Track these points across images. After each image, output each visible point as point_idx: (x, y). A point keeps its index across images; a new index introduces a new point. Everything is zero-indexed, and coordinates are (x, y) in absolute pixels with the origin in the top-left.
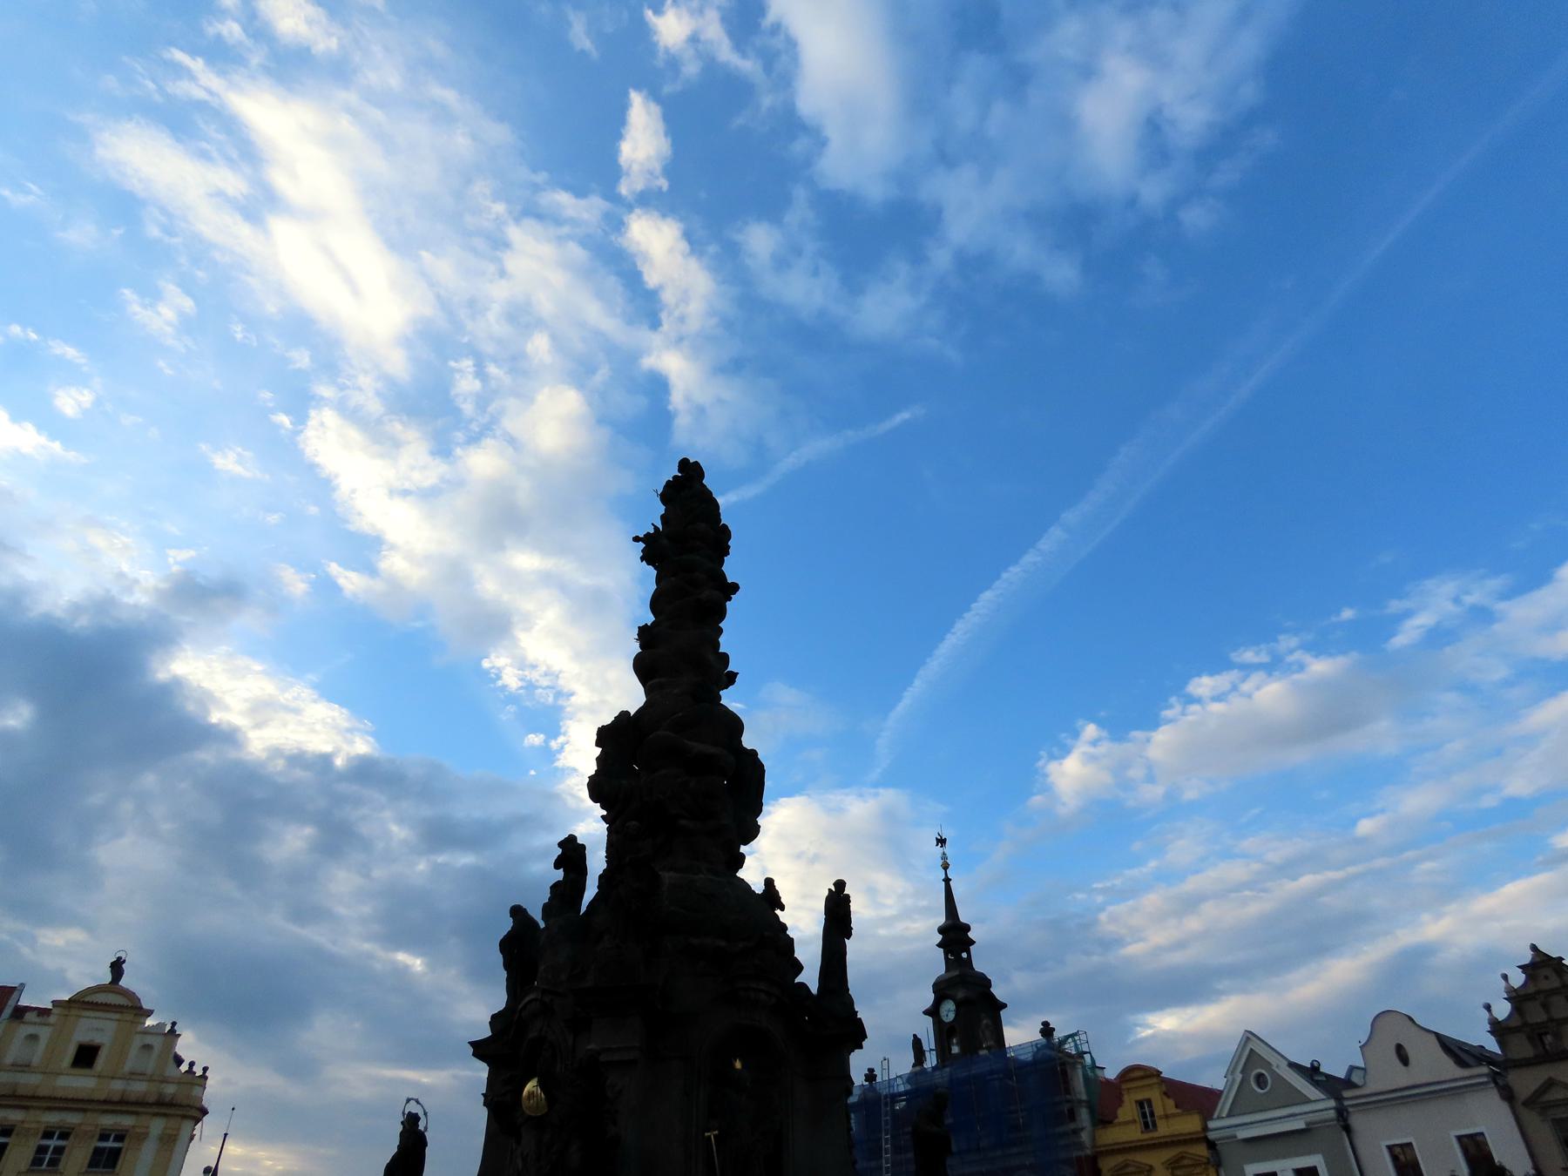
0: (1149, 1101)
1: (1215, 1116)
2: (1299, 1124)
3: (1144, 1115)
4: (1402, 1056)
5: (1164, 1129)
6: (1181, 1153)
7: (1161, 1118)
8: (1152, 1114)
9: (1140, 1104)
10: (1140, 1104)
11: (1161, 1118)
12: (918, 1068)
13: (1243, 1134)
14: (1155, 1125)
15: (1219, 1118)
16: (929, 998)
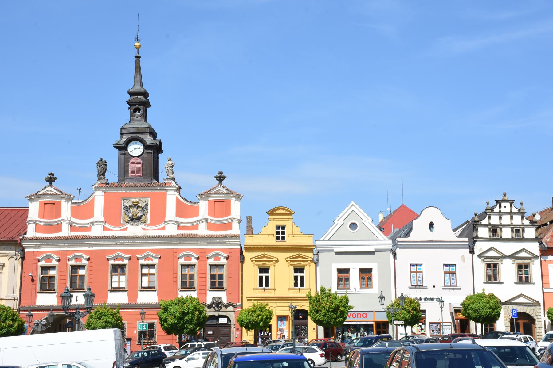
0: (283, 228)
1: (321, 239)
2: (372, 249)
3: (278, 233)
4: (432, 225)
5: (289, 241)
6: (299, 254)
7: (289, 235)
8: (283, 233)
9: (278, 227)
10: (278, 227)
11: (289, 235)
12: (104, 182)
13: (337, 250)
14: (283, 238)
15: (323, 240)
16: (117, 138)
